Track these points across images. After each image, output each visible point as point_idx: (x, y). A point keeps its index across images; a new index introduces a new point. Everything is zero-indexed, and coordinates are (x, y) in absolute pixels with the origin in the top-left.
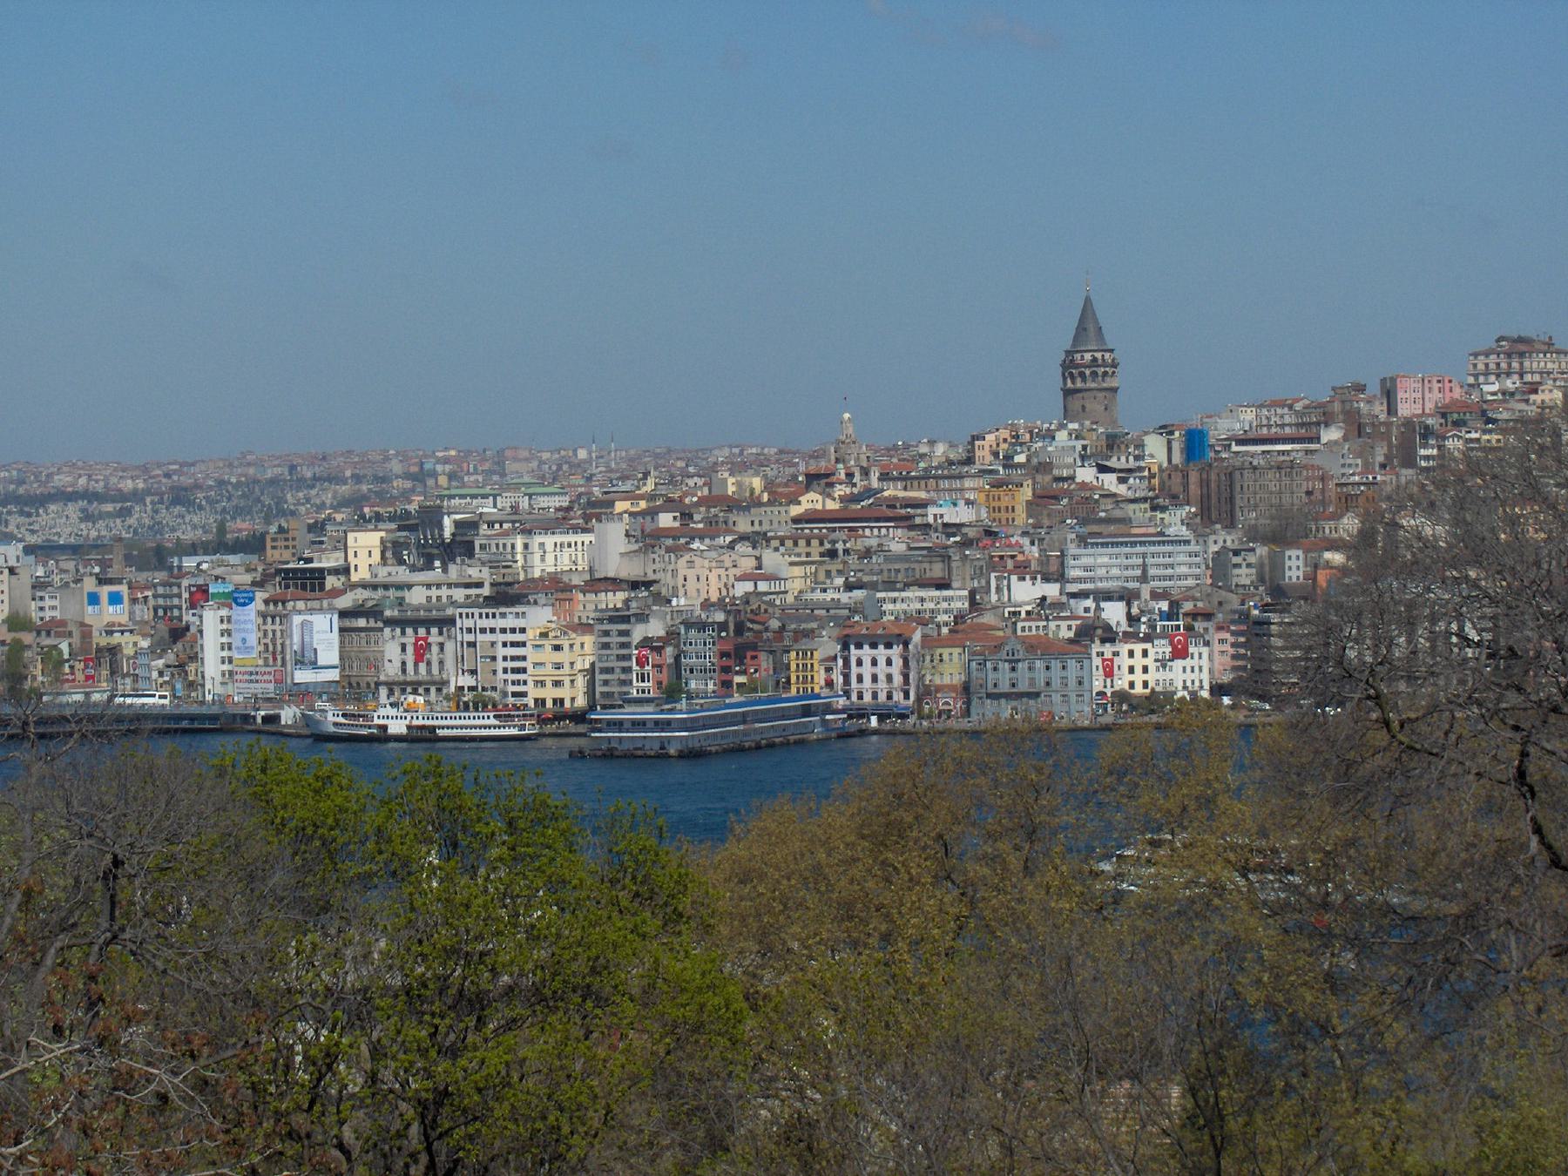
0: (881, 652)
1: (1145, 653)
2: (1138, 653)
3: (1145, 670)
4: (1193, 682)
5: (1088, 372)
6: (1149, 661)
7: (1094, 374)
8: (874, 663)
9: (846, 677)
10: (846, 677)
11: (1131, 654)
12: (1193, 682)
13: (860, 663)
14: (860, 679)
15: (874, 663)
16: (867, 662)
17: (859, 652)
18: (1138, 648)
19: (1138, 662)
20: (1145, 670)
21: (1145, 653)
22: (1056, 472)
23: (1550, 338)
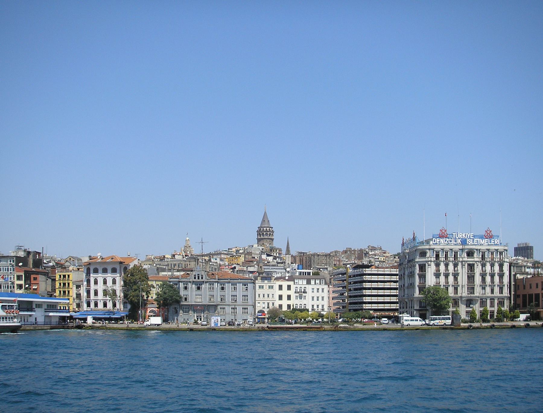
0: (109, 277)
1: (289, 287)
2: (285, 287)
3: (289, 297)
4: (318, 306)
5: (265, 233)
6: (292, 293)
8: (105, 282)
9: (88, 292)
10: (88, 292)
11: (281, 287)
12: (318, 306)
13: (96, 282)
14: (96, 293)
15: (105, 282)
16: (100, 281)
17: (95, 275)
18: (285, 284)
19: (285, 292)
20: (289, 297)
21: (289, 287)
22: (253, 256)
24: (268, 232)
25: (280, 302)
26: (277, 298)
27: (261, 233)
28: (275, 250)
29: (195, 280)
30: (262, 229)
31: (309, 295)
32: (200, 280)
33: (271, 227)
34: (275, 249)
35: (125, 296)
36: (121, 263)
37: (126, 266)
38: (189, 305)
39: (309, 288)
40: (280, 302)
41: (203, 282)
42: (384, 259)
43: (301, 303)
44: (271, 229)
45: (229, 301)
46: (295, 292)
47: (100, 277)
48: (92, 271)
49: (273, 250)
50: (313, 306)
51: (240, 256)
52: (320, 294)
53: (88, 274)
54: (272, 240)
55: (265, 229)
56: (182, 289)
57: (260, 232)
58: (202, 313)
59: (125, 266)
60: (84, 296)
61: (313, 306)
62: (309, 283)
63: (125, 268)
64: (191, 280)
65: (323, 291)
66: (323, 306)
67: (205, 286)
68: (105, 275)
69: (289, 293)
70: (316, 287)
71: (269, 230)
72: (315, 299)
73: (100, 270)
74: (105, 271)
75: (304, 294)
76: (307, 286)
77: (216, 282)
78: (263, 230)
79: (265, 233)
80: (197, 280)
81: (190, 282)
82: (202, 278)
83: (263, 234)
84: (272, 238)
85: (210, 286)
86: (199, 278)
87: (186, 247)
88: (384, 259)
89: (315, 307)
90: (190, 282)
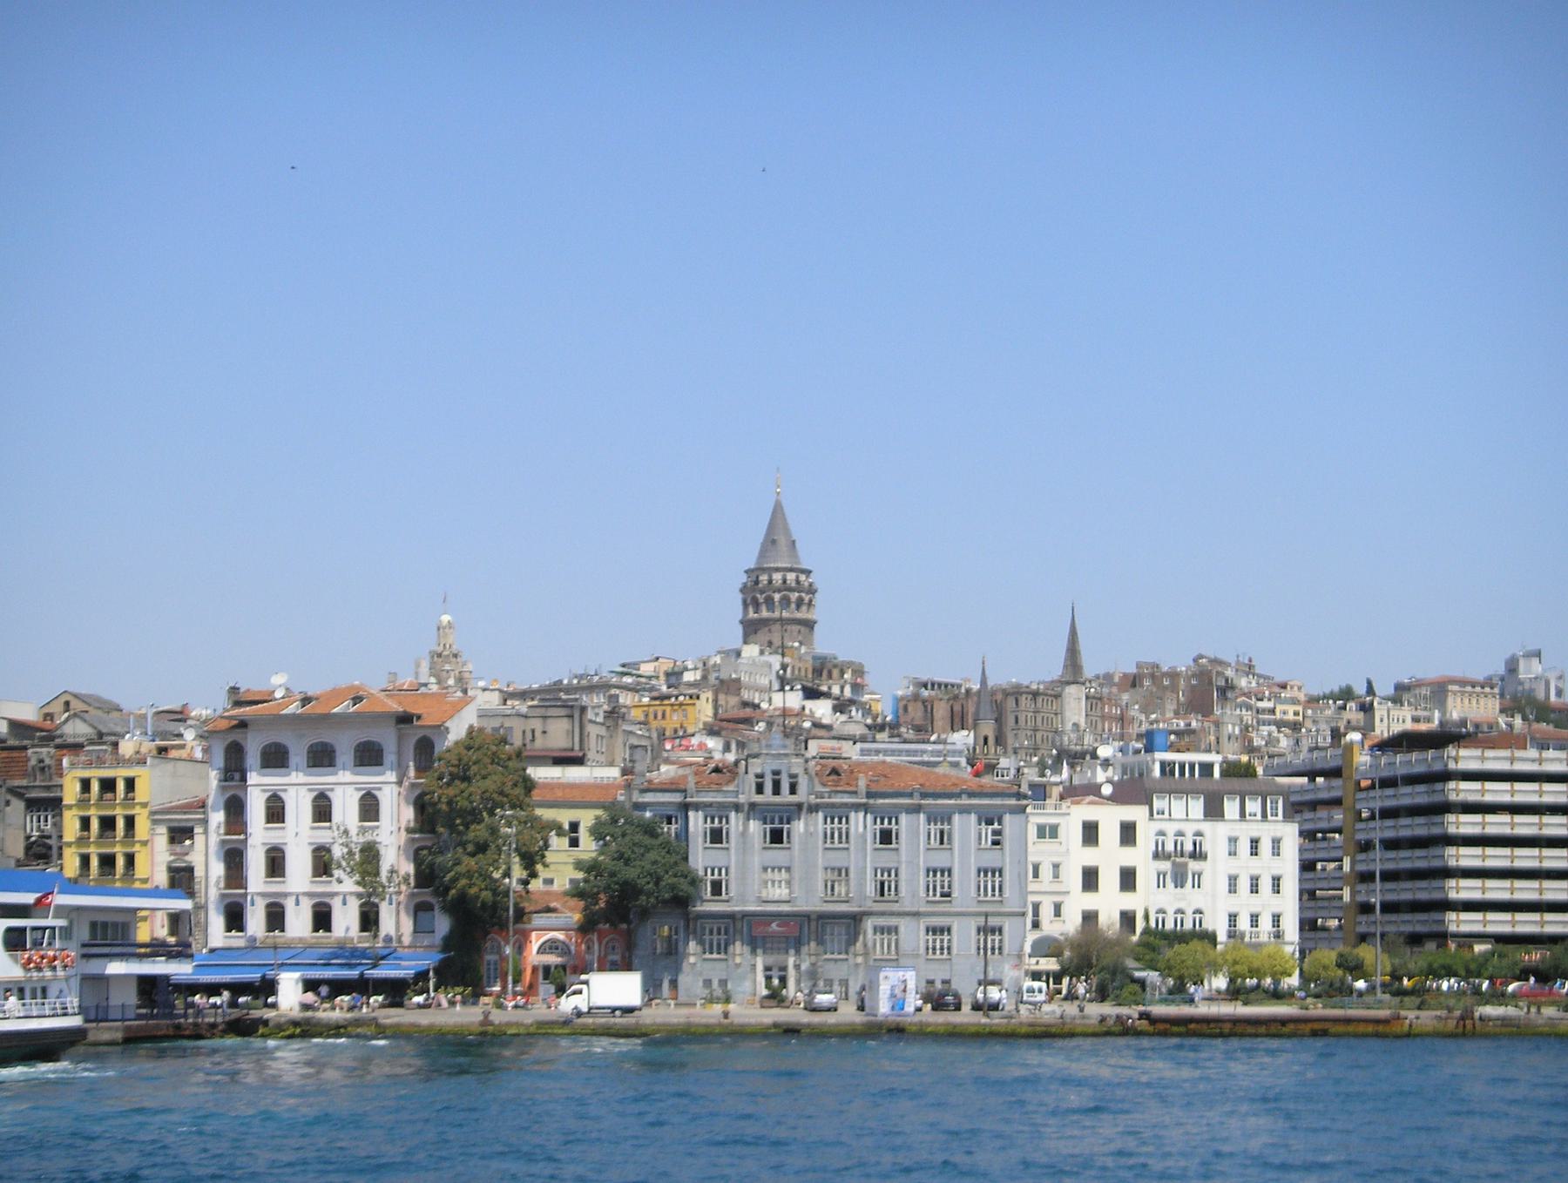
0: (345, 788)
1: (1128, 833)
2: (1109, 833)
3: (1128, 879)
4: (1254, 920)
5: (777, 597)
6: (1139, 856)
7: (786, 602)
8: (322, 810)
9: (234, 859)
10: (234, 859)
11: (1090, 833)
12: (1254, 920)
13: (276, 812)
14: (276, 863)
15: (322, 810)
16: (299, 805)
17: (273, 780)
18: (1110, 818)
19: (1109, 856)
20: (1128, 879)
21: (1128, 833)
22: (746, 695)
23: (1250, 661)
24: (791, 590)
25: (1090, 901)
26: (1077, 880)
27: (761, 598)
28: (836, 673)
29: (759, 799)
30: (764, 578)
31: (1217, 868)
32: (786, 797)
33: (803, 571)
34: (835, 666)
35: (426, 876)
36: (405, 719)
37: (428, 732)
38: (732, 916)
39: (1216, 835)
40: (1090, 901)
41: (799, 806)
42: (1296, 714)
43: (1182, 905)
44: (803, 577)
45: (914, 895)
46: (1156, 856)
47: (298, 788)
48: (253, 757)
49: (825, 673)
50: (1233, 918)
51: (698, 698)
52: (1265, 865)
53: (234, 770)
54: (809, 625)
55: (777, 577)
56: (700, 840)
57: (755, 592)
58: (792, 952)
59: (420, 734)
60: (213, 880)
61: (1233, 918)
62: (1214, 811)
63: (425, 748)
64: (742, 799)
65: (1276, 850)
66: (1276, 919)
67: (806, 825)
68: (323, 779)
69: (1129, 857)
70: (1245, 832)
71: (798, 582)
72: (1244, 884)
73: (298, 756)
74: (322, 757)
75: (1193, 866)
76: (1206, 827)
77: (857, 807)
78: (770, 582)
79: (777, 597)
80: (768, 797)
81: (737, 807)
82: (793, 790)
83: (769, 602)
84: (809, 616)
85: (829, 826)
86: (777, 790)
87: (440, 655)
88: (1296, 714)
89: (1244, 924)
90: (737, 807)
